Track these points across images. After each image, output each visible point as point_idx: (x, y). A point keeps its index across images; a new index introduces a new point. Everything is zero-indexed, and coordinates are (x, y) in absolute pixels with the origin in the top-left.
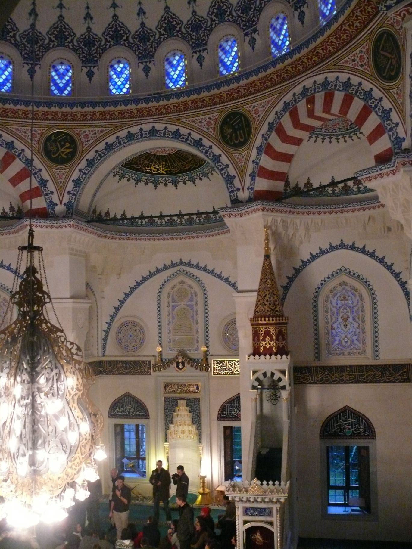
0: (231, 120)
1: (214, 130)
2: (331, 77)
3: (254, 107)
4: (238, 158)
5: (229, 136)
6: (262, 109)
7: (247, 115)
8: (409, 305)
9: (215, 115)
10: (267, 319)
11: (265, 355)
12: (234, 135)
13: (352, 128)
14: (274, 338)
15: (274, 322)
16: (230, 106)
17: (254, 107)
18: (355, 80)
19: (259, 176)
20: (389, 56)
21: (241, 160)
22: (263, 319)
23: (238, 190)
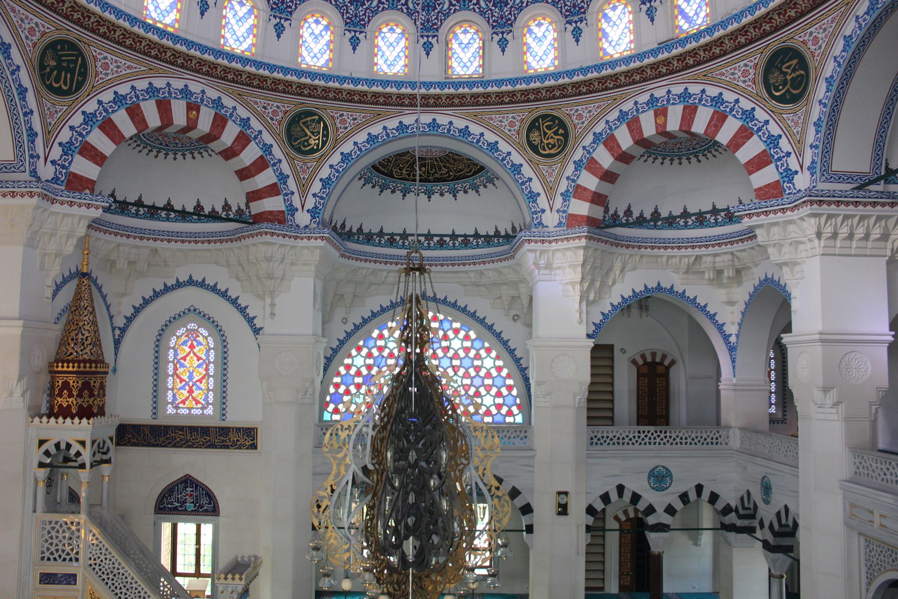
0: (63, 49)
1: (34, 47)
2: (228, 102)
3: (105, 58)
4: (49, 109)
5: (48, 70)
6: (115, 69)
7: (90, 61)
8: (116, 354)
9: (47, 25)
10: (65, 365)
11: (57, 418)
12: (55, 72)
13: (167, 145)
14: (75, 394)
15: (75, 369)
16: (74, 33)
17: (105, 58)
18: (255, 124)
19: (80, 153)
20: (309, 133)
21: (52, 115)
22: (71, 365)
23: (38, 157)
